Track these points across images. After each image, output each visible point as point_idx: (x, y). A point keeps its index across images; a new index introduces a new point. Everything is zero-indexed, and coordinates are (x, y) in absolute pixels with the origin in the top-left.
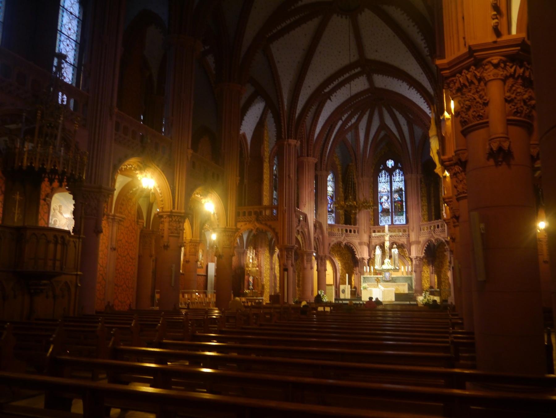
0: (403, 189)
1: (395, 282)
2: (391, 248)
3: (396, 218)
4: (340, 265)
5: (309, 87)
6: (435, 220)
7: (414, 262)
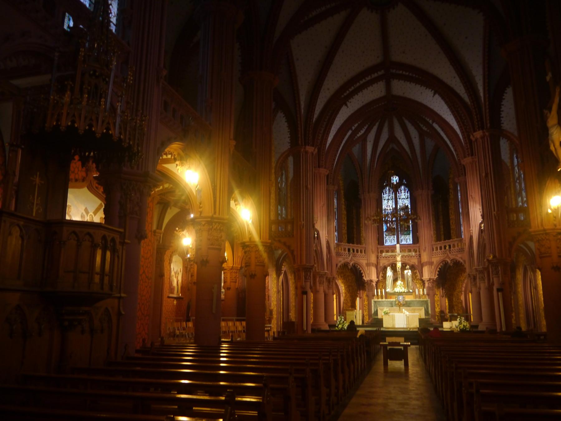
0: (409, 206)
1: (409, 306)
2: (403, 268)
3: (402, 237)
4: (343, 288)
5: (328, 89)
6: (445, 240)
7: (427, 285)
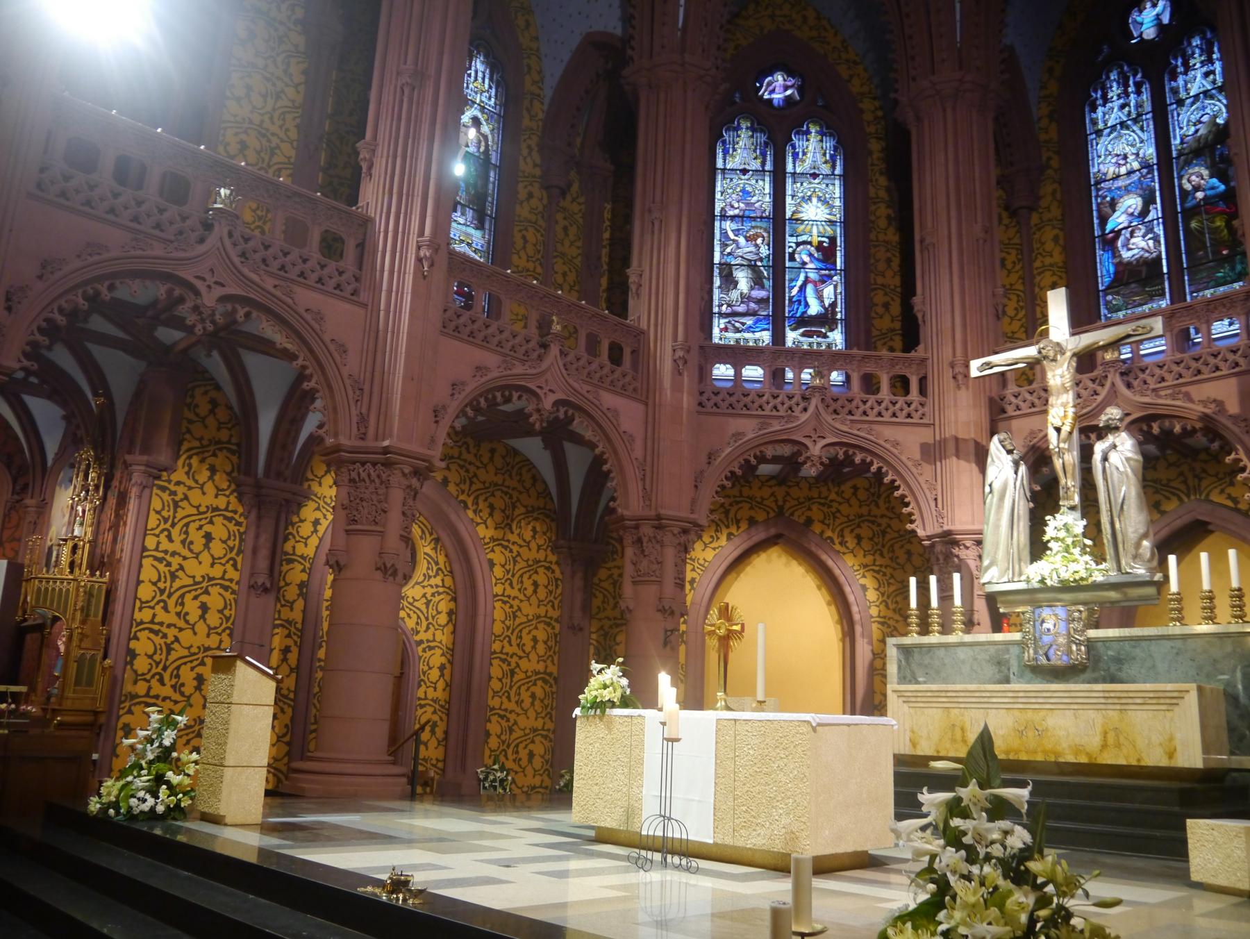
2: (1089, 431)
4: (872, 595)
